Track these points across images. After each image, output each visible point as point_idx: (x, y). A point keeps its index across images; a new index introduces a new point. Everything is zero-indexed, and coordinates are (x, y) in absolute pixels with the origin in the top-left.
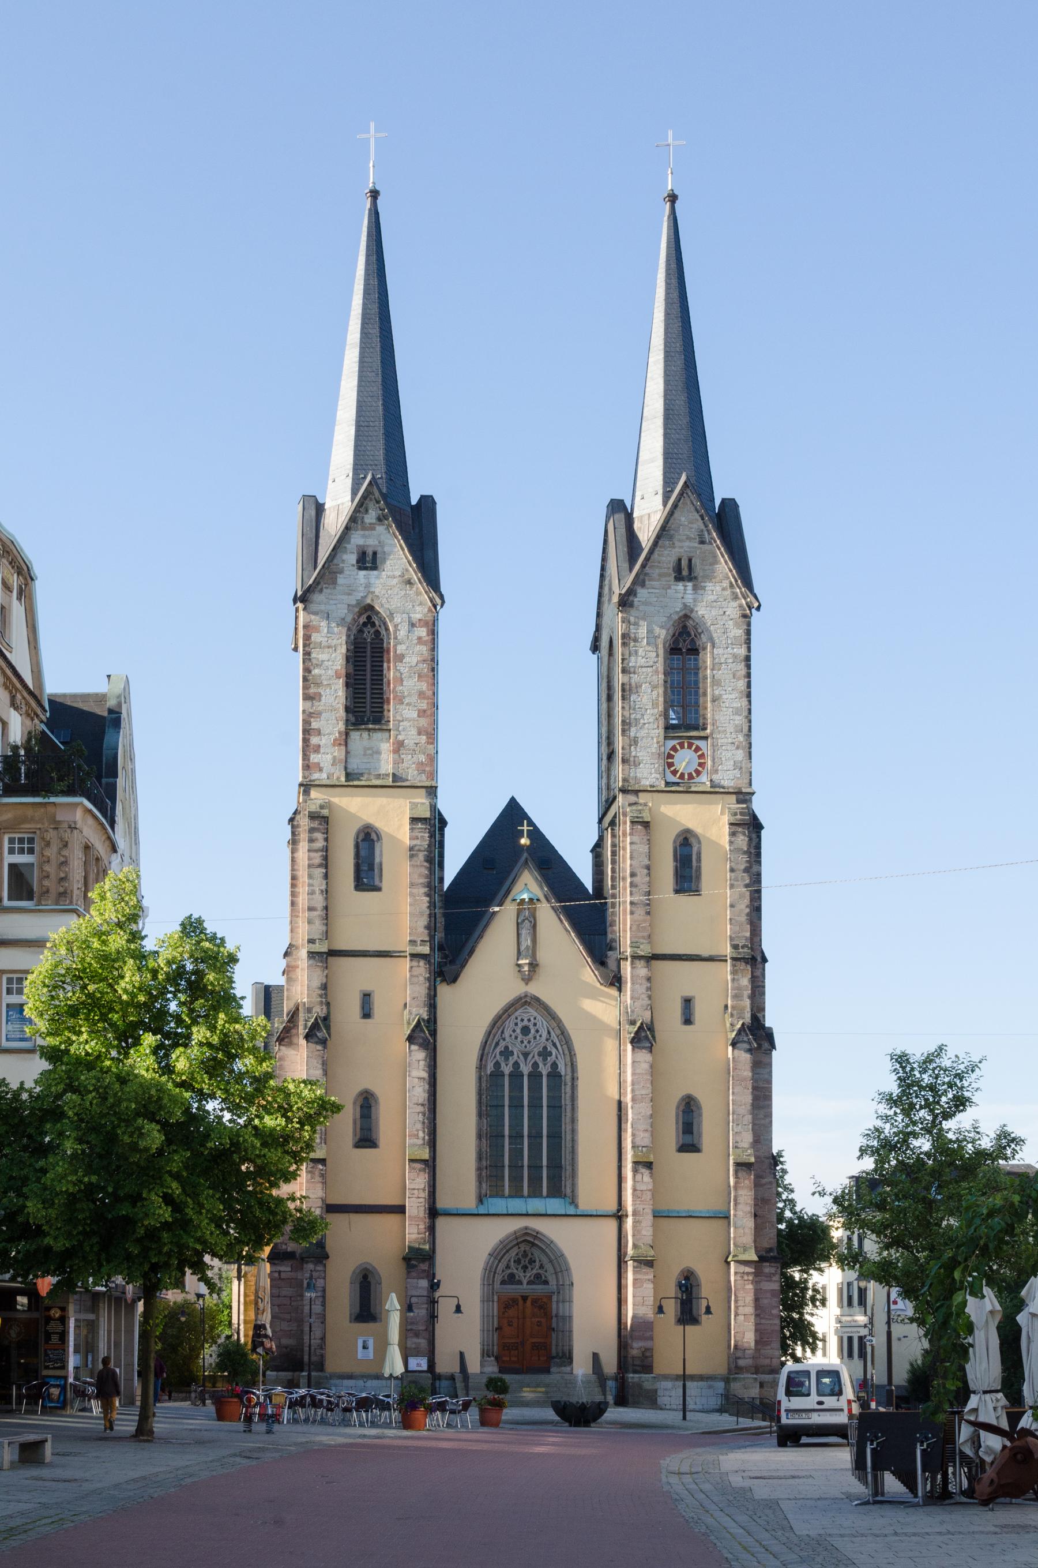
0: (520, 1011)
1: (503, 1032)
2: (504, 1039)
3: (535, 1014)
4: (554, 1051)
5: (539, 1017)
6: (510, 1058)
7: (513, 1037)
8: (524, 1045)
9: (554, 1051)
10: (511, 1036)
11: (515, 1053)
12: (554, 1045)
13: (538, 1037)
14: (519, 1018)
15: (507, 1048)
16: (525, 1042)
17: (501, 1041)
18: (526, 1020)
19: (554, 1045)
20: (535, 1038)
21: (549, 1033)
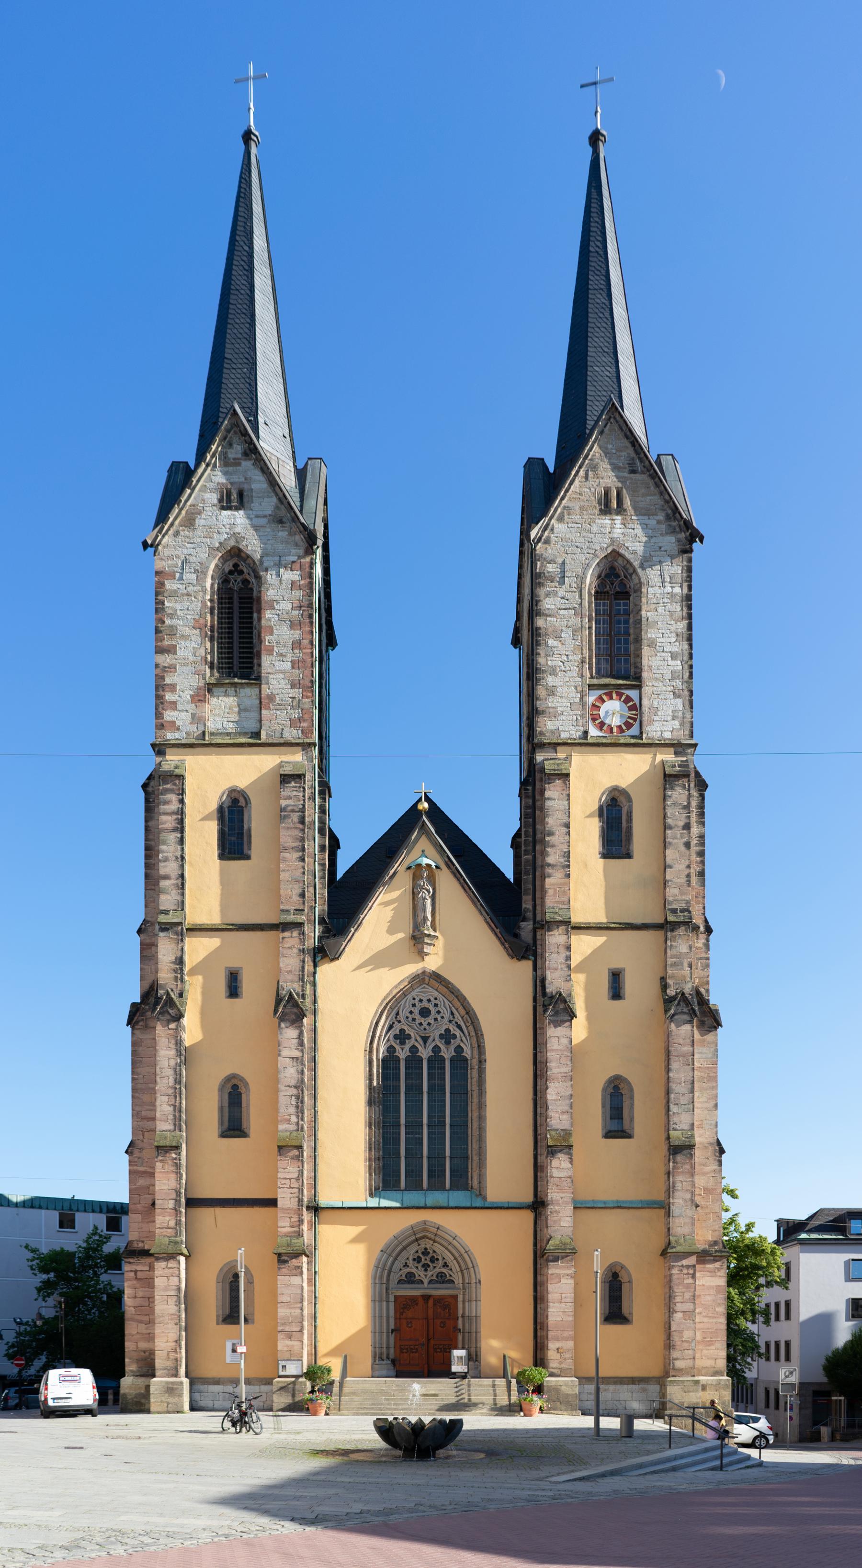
0: (418, 990)
1: (397, 1014)
2: (399, 1022)
3: (436, 994)
4: (458, 1033)
5: (440, 997)
6: (407, 1041)
7: (410, 1019)
8: (422, 1027)
9: (458, 1033)
10: (407, 1017)
11: (413, 1036)
12: (459, 1027)
13: (439, 1018)
14: (417, 999)
15: (402, 1031)
16: (425, 1024)
17: (396, 1023)
18: (425, 999)
19: (459, 1027)
20: (436, 1019)
21: (452, 1013)
